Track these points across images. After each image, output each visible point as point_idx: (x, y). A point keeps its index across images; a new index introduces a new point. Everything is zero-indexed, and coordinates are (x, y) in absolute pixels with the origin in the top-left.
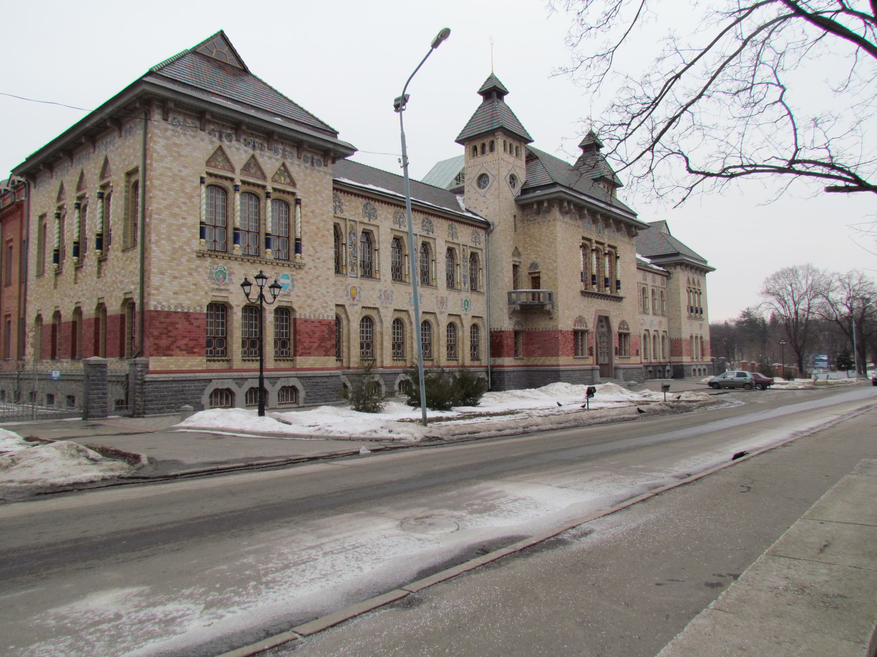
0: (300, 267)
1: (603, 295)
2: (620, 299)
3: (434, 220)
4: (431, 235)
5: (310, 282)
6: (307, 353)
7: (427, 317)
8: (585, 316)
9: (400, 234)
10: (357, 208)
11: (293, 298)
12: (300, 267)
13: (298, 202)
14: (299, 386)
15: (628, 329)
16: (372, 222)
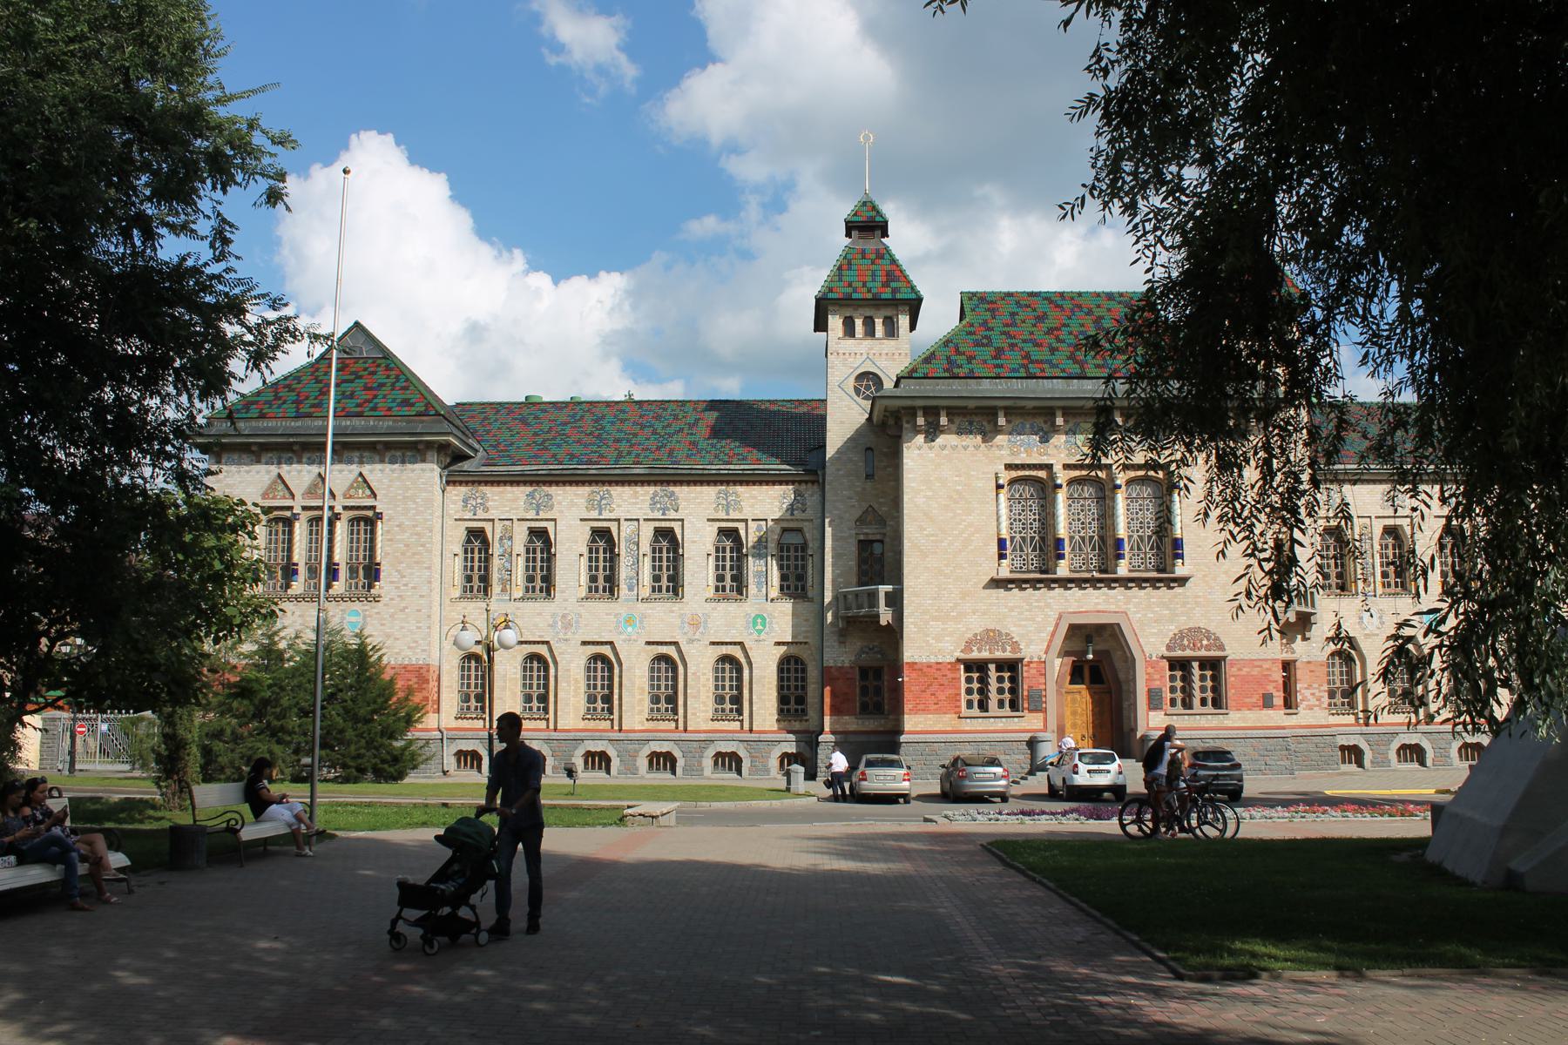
2: (1182, 581)
3: (682, 492)
4: (672, 514)
5: (392, 616)
9: (605, 524)
10: (515, 500)
12: (376, 599)
13: (379, 516)
15: (1222, 648)
16: (542, 515)
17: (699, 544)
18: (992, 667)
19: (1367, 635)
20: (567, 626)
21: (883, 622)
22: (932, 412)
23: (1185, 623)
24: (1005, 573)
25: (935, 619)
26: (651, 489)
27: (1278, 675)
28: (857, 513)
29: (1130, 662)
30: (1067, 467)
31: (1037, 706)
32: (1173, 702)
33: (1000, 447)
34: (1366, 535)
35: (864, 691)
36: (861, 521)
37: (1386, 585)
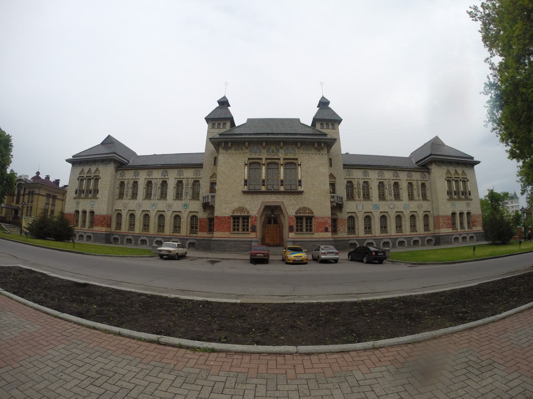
0: (97, 198)
1: (270, 192)
2: (301, 193)
3: (169, 171)
4: (166, 177)
6: (96, 226)
7: (162, 213)
8: (248, 207)
11: (94, 208)
12: (97, 198)
14: (92, 236)
15: (313, 213)
17: (172, 184)
18: (241, 218)
19: (359, 212)
20: (139, 206)
21: (210, 204)
22: (226, 143)
23: (301, 205)
24: (246, 189)
25: (225, 203)
26: (162, 170)
27: (330, 222)
28: (211, 175)
29: (284, 217)
30: (266, 159)
31: (254, 230)
32: (297, 230)
33: (247, 153)
34: (358, 184)
35: (210, 225)
36: (211, 177)
37: (364, 198)
